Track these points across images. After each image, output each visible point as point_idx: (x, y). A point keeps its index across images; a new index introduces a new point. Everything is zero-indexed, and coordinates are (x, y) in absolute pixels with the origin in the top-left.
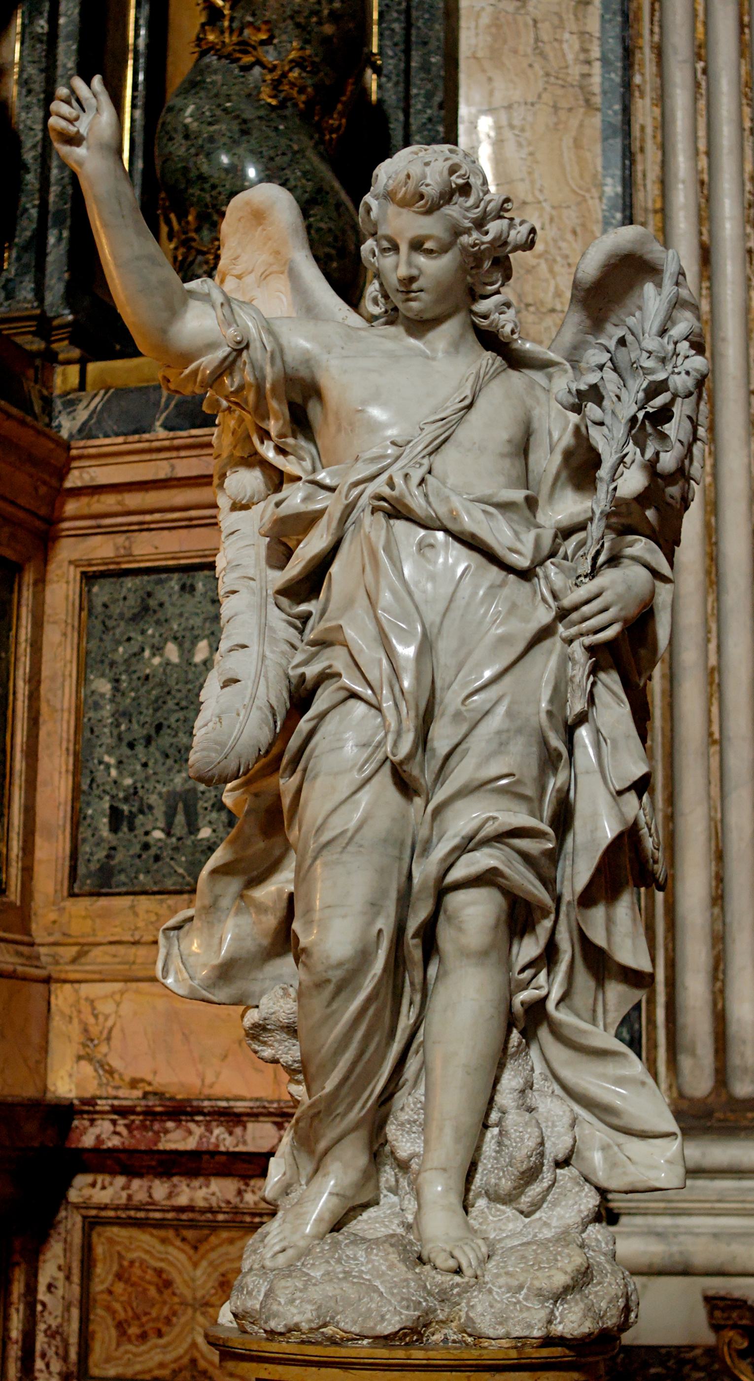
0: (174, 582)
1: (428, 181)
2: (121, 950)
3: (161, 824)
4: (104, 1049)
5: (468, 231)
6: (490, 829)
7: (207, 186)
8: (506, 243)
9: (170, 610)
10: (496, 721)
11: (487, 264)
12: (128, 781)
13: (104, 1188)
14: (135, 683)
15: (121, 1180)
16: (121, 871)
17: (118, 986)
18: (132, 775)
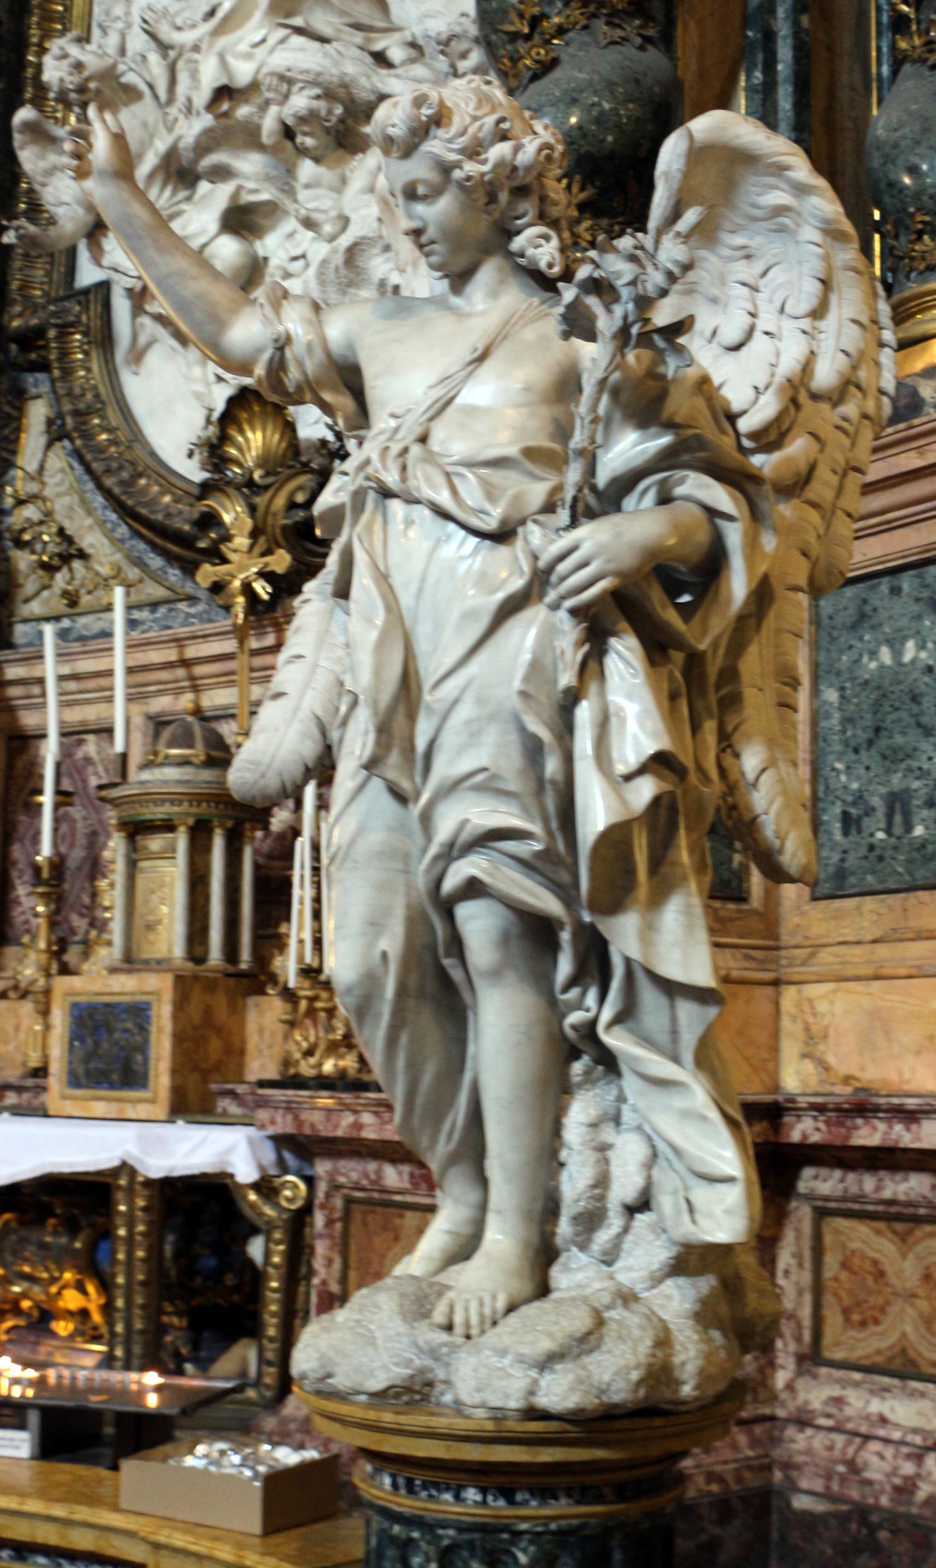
0: (884, 585)
1: (396, 121)
2: (842, 949)
3: (882, 825)
4: (822, 1047)
5: (458, 165)
6: (465, 836)
7: (895, 192)
9: (883, 614)
10: (465, 711)
11: (504, 197)
12: (855, 786)
13: (825, 1180)
14: (858, 689)
15: (838, 1173)
16: (853, 873)
17: (830, 986)
18: (858, 778)
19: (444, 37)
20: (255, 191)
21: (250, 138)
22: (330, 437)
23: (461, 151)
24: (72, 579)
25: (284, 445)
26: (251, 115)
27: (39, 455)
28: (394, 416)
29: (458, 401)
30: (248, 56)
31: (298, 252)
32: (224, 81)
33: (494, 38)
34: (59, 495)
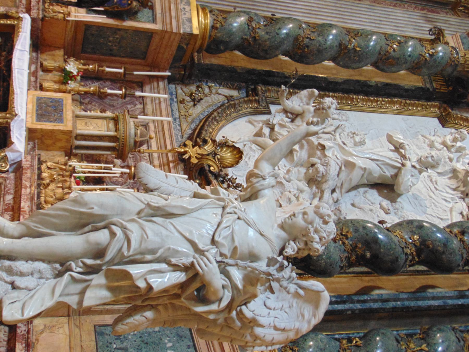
0: (191, 343)
1: (324, 209)
2: (79, 336)
3: (118, 347)
4: (48, 331)
5: (313, 227)
6: (128, 232)
8: (312, 242)
9: (181, 343)
11: (304, 239)
12: (130, 337)
13: (4, 335)
14: (159, 336)
15: (6, 339)
16: (103, 338)
17: (68, 333)
18: (132, 338)
19: (340, 209)
20: (297, 156)
21: (311, 155)
22: (229, 177)
23: (316, 228)
24: (188, 102)
25: (227, 164)
26: (318, 155)
27: (223, 93)
28: (245, 209)
29: (250, 228)
30: (333, 155)
31: (280, 168)
32: (327, 148)
33: (341, 224)
34: (211, 98)
